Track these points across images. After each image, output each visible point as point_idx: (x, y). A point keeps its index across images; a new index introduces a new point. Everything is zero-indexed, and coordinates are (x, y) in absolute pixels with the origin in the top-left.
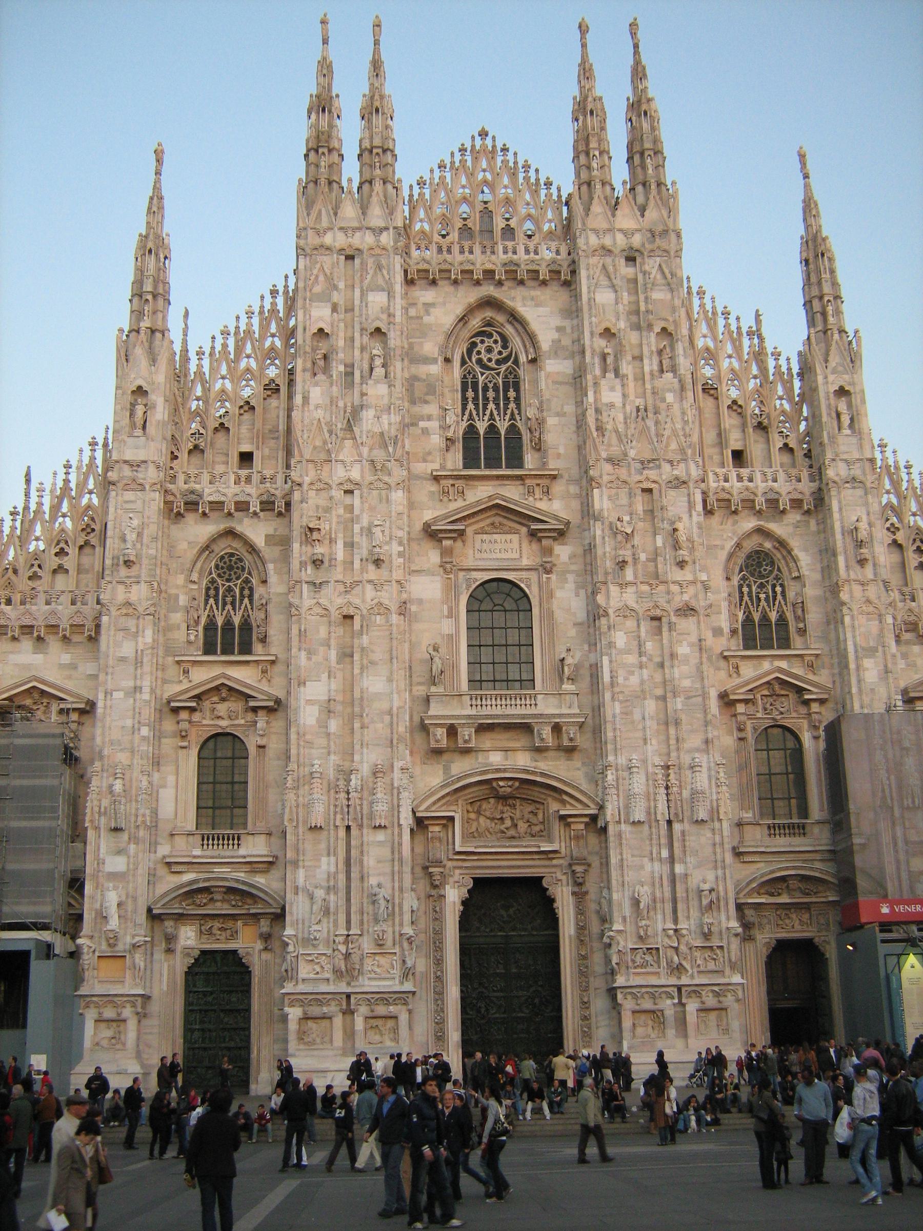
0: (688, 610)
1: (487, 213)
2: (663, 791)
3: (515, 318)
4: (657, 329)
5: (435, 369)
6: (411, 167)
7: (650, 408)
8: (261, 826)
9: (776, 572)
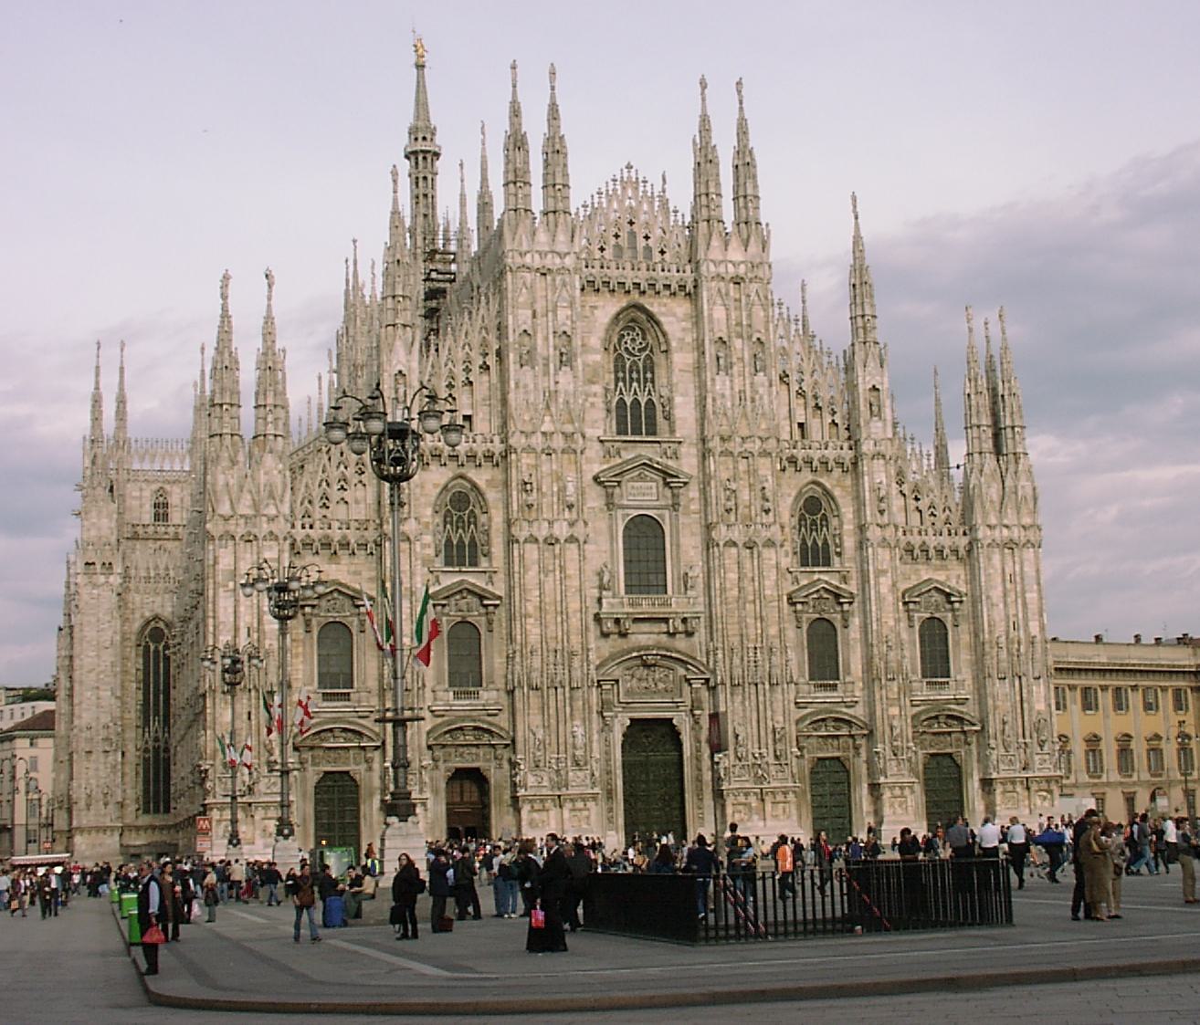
0: (770, 543)
1: (633, 235)
2: (752, 664)
4: (754, 339)
5: (598, 357)
6: (579, 197)
7: (748, 398)
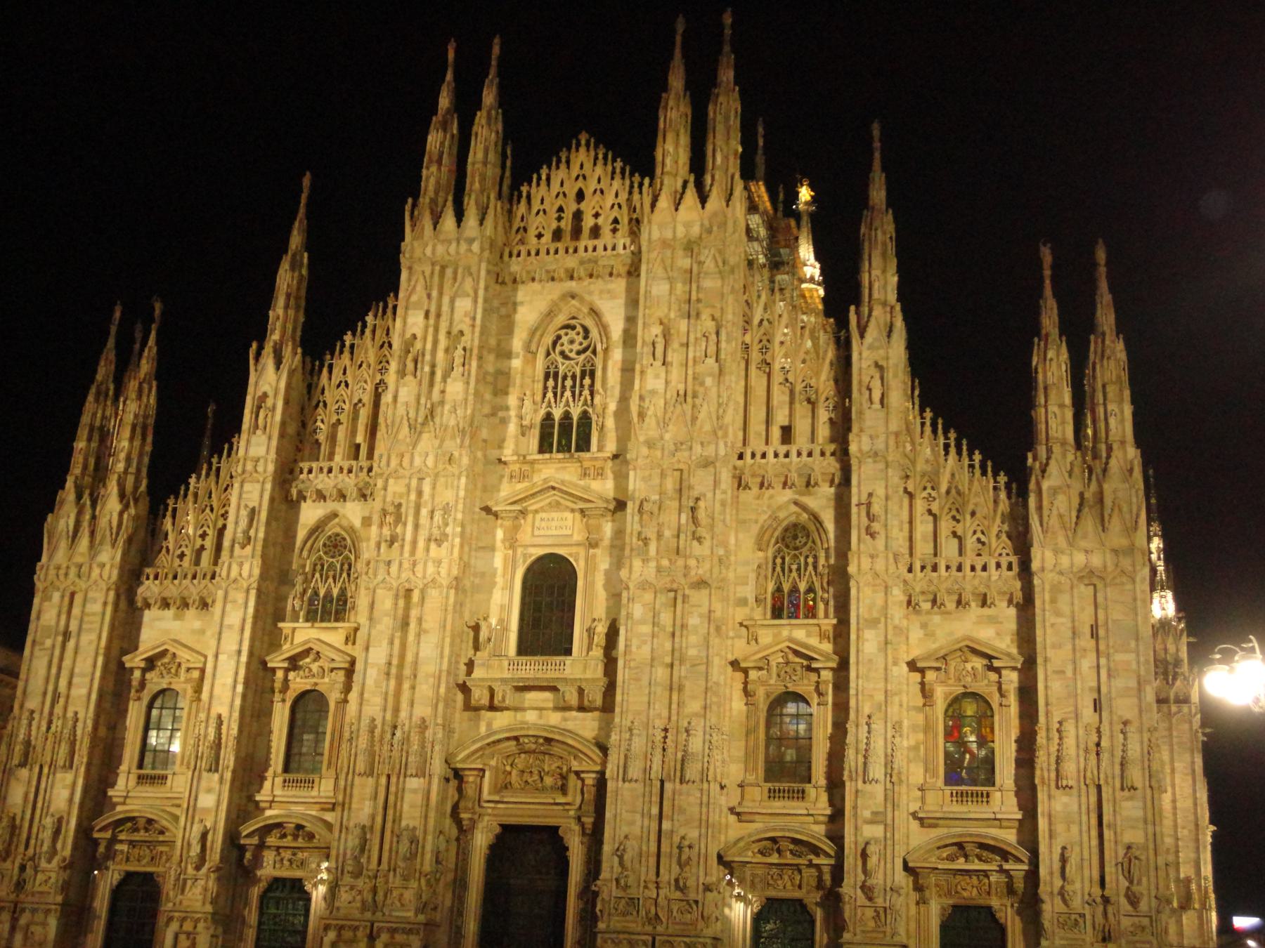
0: (701, 584)
2: (659, 751)
3: (594, 312)
7: (689, 393)
8: (332, 771)
9: (810, 544)
